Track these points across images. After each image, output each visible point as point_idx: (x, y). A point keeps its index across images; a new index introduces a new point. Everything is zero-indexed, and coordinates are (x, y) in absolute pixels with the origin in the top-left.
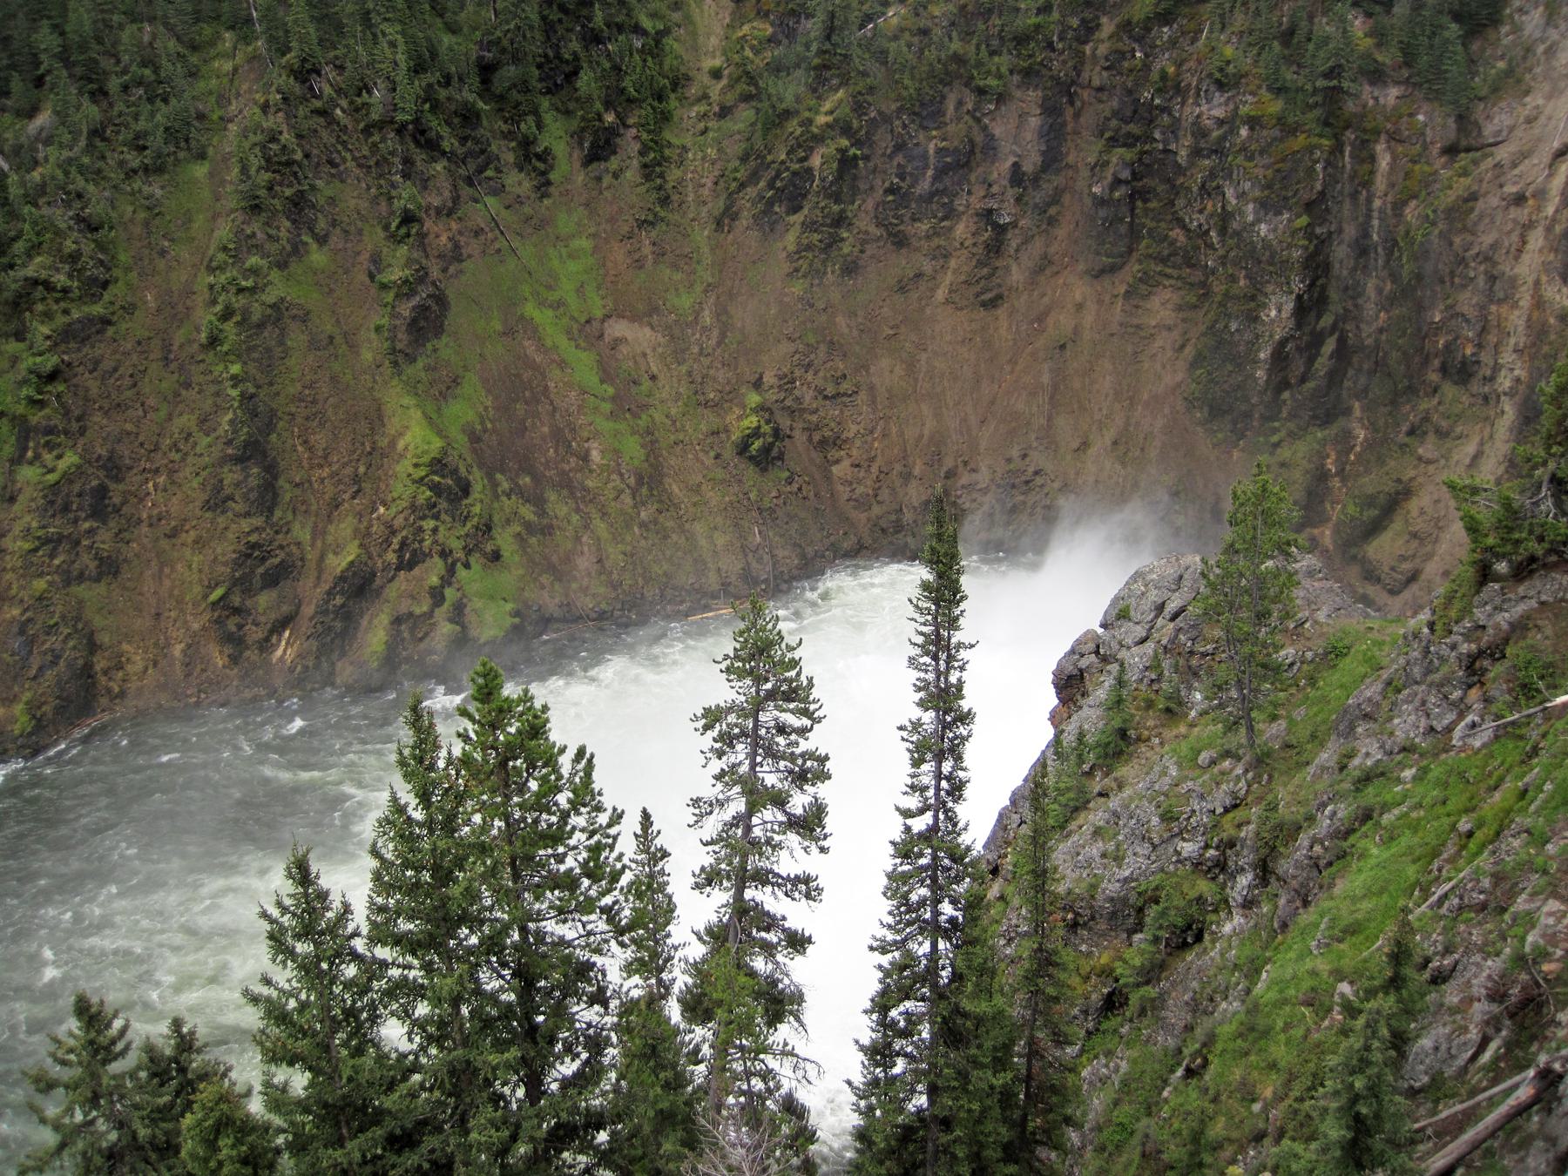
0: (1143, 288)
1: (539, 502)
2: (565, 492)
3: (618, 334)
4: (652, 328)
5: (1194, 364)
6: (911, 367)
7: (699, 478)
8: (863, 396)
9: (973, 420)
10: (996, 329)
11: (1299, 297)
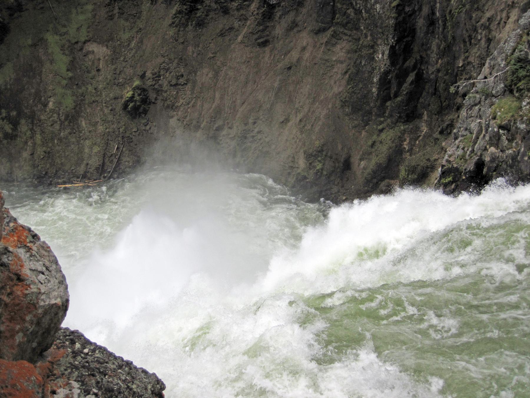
0: (334, 40)
1: (15, 124)
3: (90, 49)
4: (107, 48)
5: (348, 83)
6: (217, 74)
7: (98, 120)
8: (189, 85)
9: (239, 102)
10: (263, 58)
11: (392, 48)
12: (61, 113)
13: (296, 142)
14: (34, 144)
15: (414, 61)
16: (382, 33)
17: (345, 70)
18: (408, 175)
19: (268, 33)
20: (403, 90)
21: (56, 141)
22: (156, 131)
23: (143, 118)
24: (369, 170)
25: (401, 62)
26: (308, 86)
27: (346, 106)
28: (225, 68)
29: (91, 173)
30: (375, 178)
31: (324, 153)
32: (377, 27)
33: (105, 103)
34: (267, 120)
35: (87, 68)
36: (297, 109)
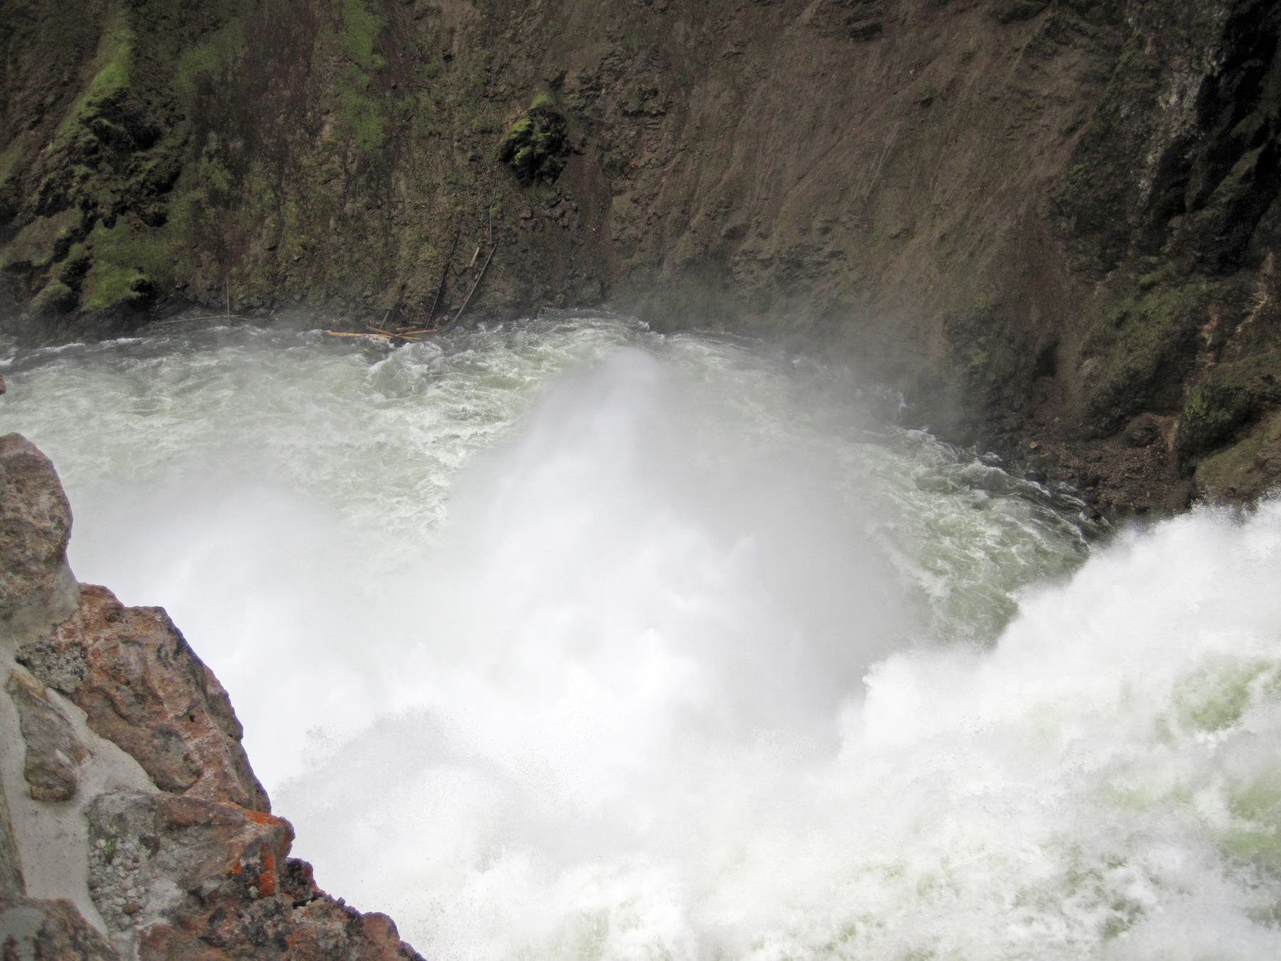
0: (1050, 44)
1: (239, 170)
2: (274, 165)
7: (439, 180)
8: (671, 119)
11: (1211, 81)
12: (349, 154)
13: (926, 291)
14: (281, 224)
15: (1262, 121)
16: (1189, 41)
17: (1070, 124)
18: (1209, 409)
19: (880, 8)
20: (1221, 194)
21: (332, 222)
22: (575, 223)
23: (548, 186)
24: (1103, 385)
25: (1226, 117)
26: (970, 153)
27: (1061, 214)
28: (763, 85)
29: (411, 310)
30: (1117, 405)
31: (996, 327)
32: (1174, 22)
33: (459, 141)
34: (856, 226)
35: (421, 50)
36: (937, 207)
